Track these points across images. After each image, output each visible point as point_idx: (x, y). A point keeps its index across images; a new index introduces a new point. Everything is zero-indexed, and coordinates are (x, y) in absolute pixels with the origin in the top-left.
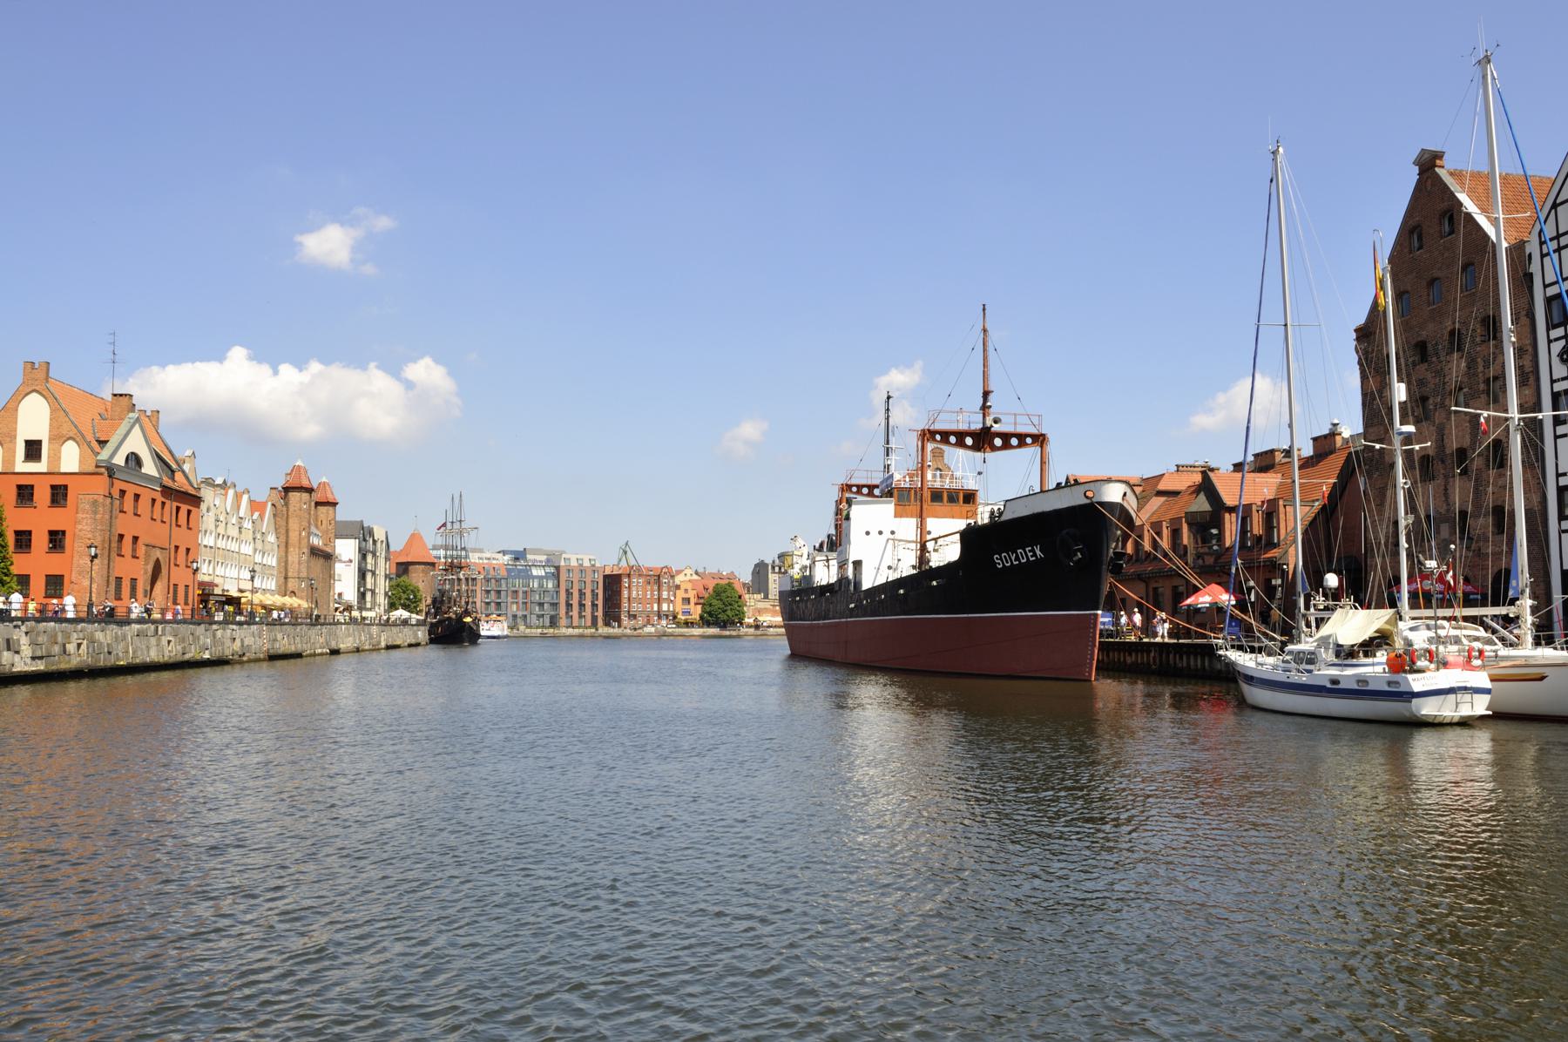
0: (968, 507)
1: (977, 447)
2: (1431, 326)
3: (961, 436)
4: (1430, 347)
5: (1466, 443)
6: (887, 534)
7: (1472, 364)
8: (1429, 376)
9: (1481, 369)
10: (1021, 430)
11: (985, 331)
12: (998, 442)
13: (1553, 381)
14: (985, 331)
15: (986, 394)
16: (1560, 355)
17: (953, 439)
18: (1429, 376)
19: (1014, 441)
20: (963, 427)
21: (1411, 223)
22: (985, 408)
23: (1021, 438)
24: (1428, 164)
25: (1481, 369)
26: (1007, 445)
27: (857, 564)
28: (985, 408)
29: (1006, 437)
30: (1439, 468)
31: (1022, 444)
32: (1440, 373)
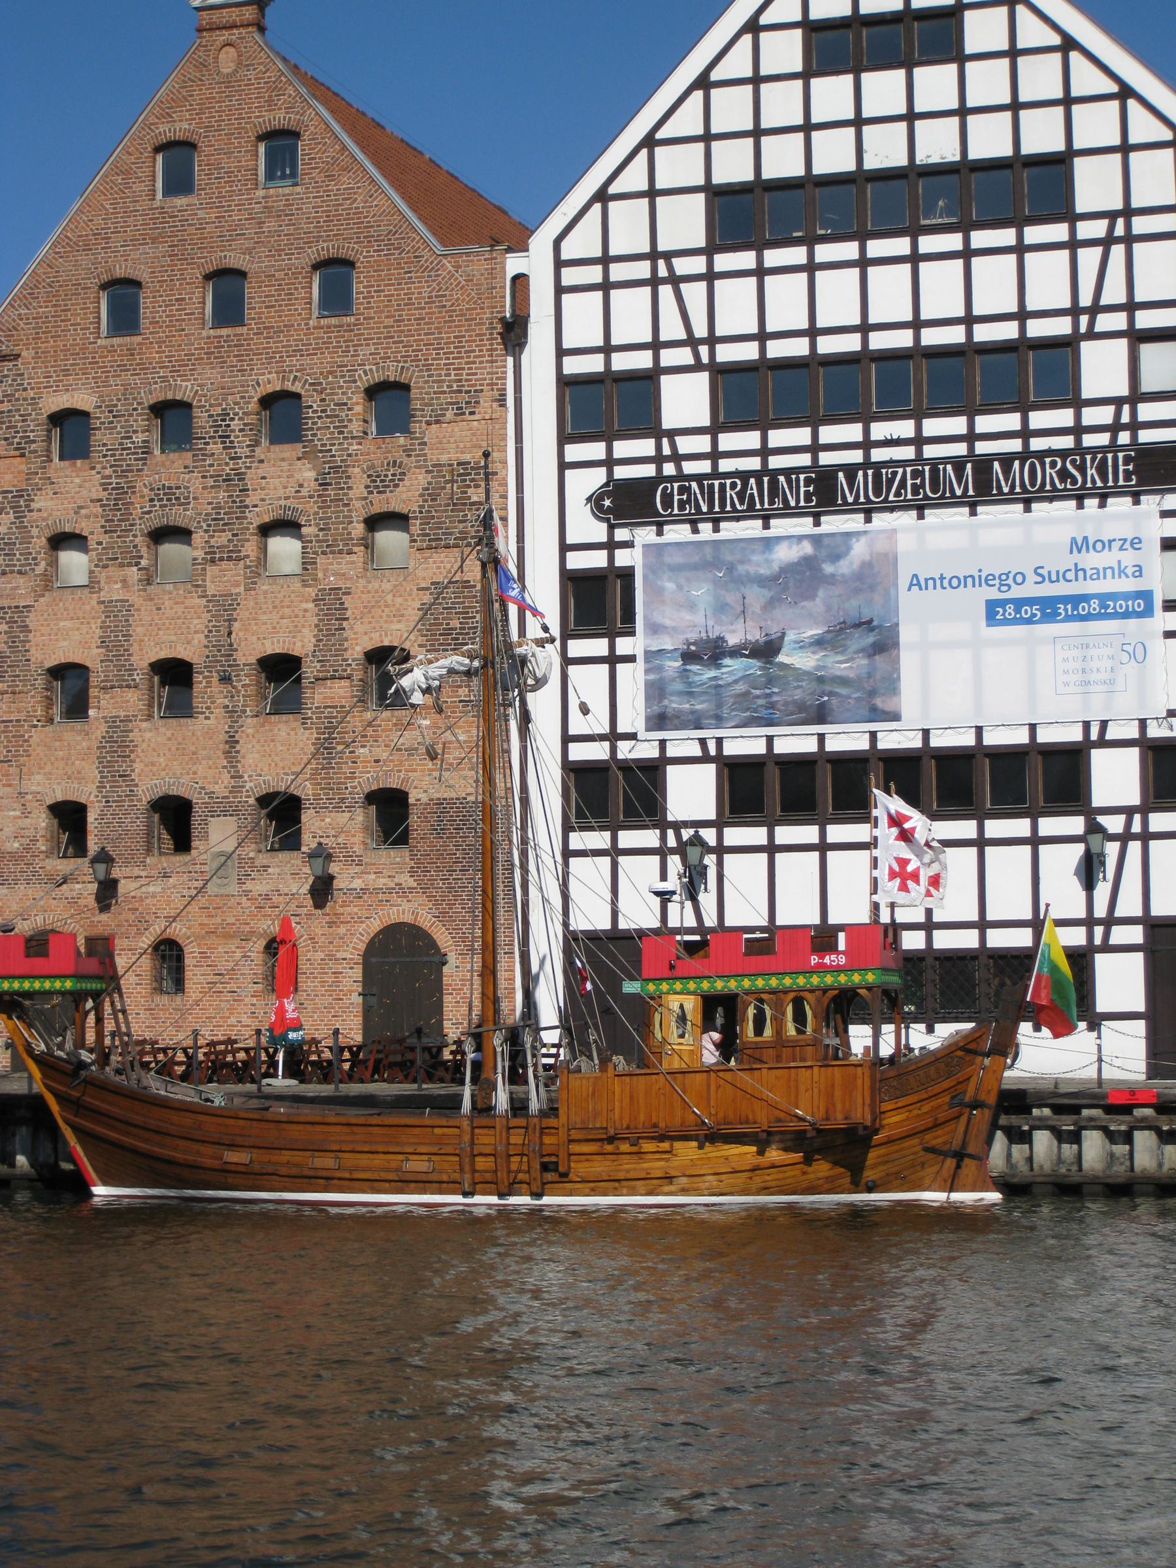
2: (211, 375)
4: (201, 419)
5: (302, 643)
7: (331, 477)
8: (195, 483)
9: (358, 488)
13: (565, 548)
16: (595, 500)
18: (195, 483)
21: (166, 131)
25: (358, 488)
30: (204, 686)
32: (235, 481)
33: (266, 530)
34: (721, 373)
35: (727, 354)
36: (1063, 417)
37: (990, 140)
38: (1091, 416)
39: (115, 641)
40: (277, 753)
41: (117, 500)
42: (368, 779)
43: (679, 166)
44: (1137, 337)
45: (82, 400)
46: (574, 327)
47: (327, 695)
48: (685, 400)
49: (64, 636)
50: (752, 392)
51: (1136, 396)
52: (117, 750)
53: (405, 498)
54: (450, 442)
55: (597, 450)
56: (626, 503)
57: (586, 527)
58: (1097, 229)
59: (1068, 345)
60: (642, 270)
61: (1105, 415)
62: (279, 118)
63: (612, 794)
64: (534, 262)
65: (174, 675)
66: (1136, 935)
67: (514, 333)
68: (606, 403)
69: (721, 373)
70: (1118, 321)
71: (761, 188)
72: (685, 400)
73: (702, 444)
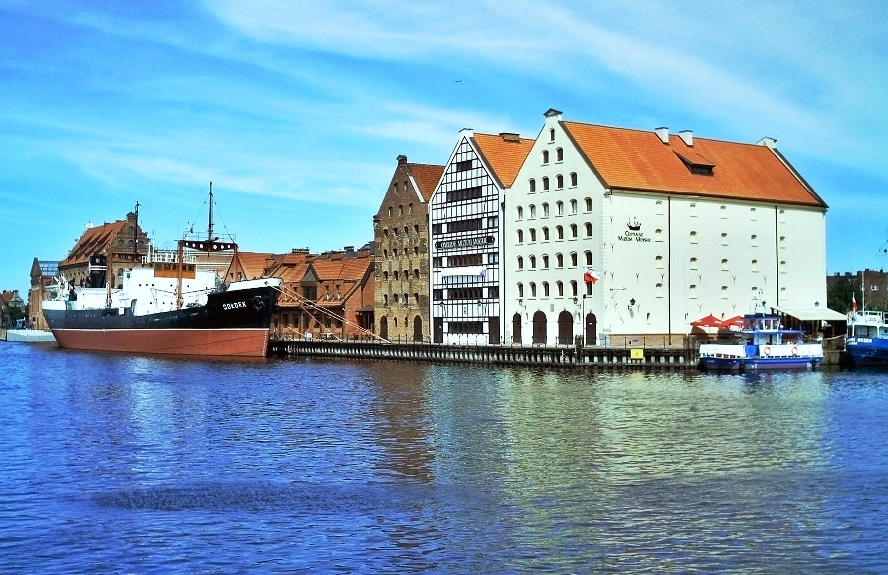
0: (190, 273)
1: (204, 250)
3: (198, 244)
5: (408, 269)
6: (150, 286)
10: (226, 242)
11: (211, 194)
12: (215, 247)
14: (211, 194)
15: (210, 225)
17: (194, 245)
19: (222, 247)
20: (200, 240)
22: (210, 233)
23: (226, 245)
24: (402, 160)
26: (219, 249)
27: (134, 301)
28: (210, 233)
29: (219, 245)
31: (226, 248)
32: (401, 242)
33: (406, 249)
34: (448, 223)
35: (450, 220)
36: (480, 232)
37: (474, 185)
38: (484, 231)
39: (390, 269)
40: (406, 288)
41: (390, 245)
42: (414, 292)
43: (444, 188)
44: (489, 218)
45: (387, 228)
46: (435, 215)
47: (411, 277)
48: (444, 228)
49: (385, 268)
50: (455, 226)
51: (489, 228)
52: (390, 286)
53: (418, 245)
54: (423, 235)
55: (435, 237)
56: (438, 245)
57: (435, 251)
58: (484, 199)
59: (481, 219)
60: (439, 206)
61: (484, 231)
62: (406, 179)
63: (438, 293)
64: (430, 205)
65: (396, 273)
66: (487, 319)
67: (428, 216)
68: (437, 228)
69: (448, 223)
70: (486, 215)
71: (452, 192)
72: (444, 228)
73: (445, 236)
